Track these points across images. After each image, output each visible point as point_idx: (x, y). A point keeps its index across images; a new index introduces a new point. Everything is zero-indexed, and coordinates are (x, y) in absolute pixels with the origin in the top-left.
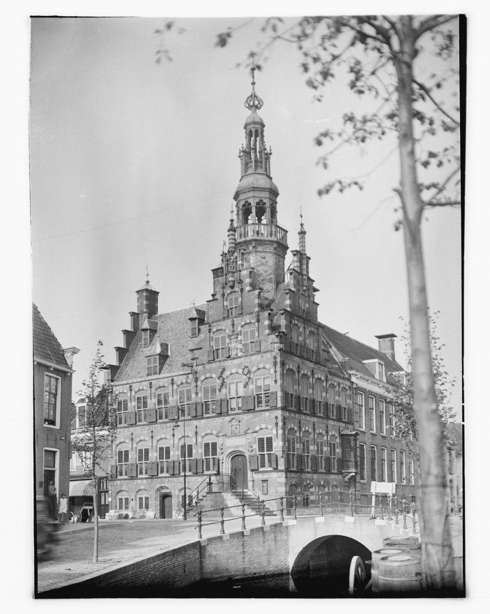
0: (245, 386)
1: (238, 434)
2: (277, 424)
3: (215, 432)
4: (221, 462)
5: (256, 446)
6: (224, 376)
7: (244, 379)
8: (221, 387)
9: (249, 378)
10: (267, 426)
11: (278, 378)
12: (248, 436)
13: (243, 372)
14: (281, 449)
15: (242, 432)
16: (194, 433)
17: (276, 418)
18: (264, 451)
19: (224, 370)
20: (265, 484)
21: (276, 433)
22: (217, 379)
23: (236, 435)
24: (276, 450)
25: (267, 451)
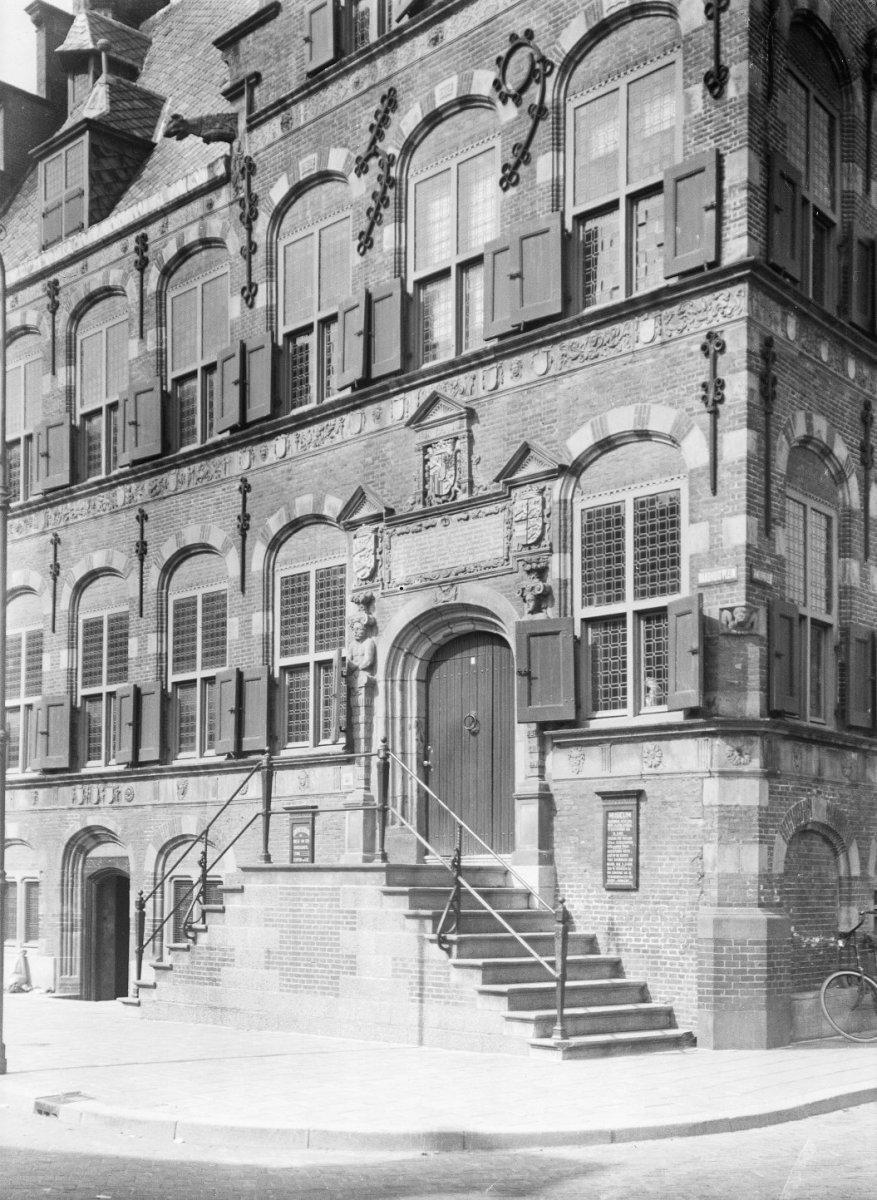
0: (509, 179)
1: (462, 497)
2: (714, 394)
3: (333, 506)
4: (362, 678)
5: (567, 567)
6: (391, 146)
7: (506, 131)
8: (375, 218)
9: (539, 113)
10: (642, 415)
11: (736, 46)
12: (525, 500)
13: (497, 85)
14: (735, 571)
15: (485, 480)
16: (233, 523)
17: (713, 347)
18: (620, 597)
19: (391, 101)
20: (621, 821)
21: (704, 458)
22: (352, 177)
23: (450, 507)
24: (703, 578)
25: (641, 594)
